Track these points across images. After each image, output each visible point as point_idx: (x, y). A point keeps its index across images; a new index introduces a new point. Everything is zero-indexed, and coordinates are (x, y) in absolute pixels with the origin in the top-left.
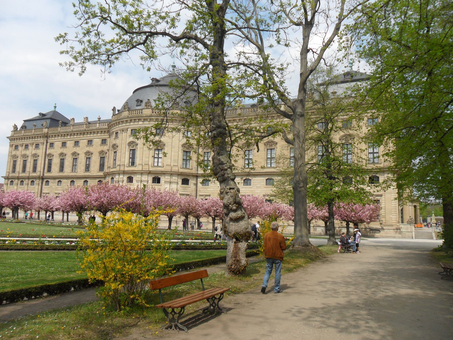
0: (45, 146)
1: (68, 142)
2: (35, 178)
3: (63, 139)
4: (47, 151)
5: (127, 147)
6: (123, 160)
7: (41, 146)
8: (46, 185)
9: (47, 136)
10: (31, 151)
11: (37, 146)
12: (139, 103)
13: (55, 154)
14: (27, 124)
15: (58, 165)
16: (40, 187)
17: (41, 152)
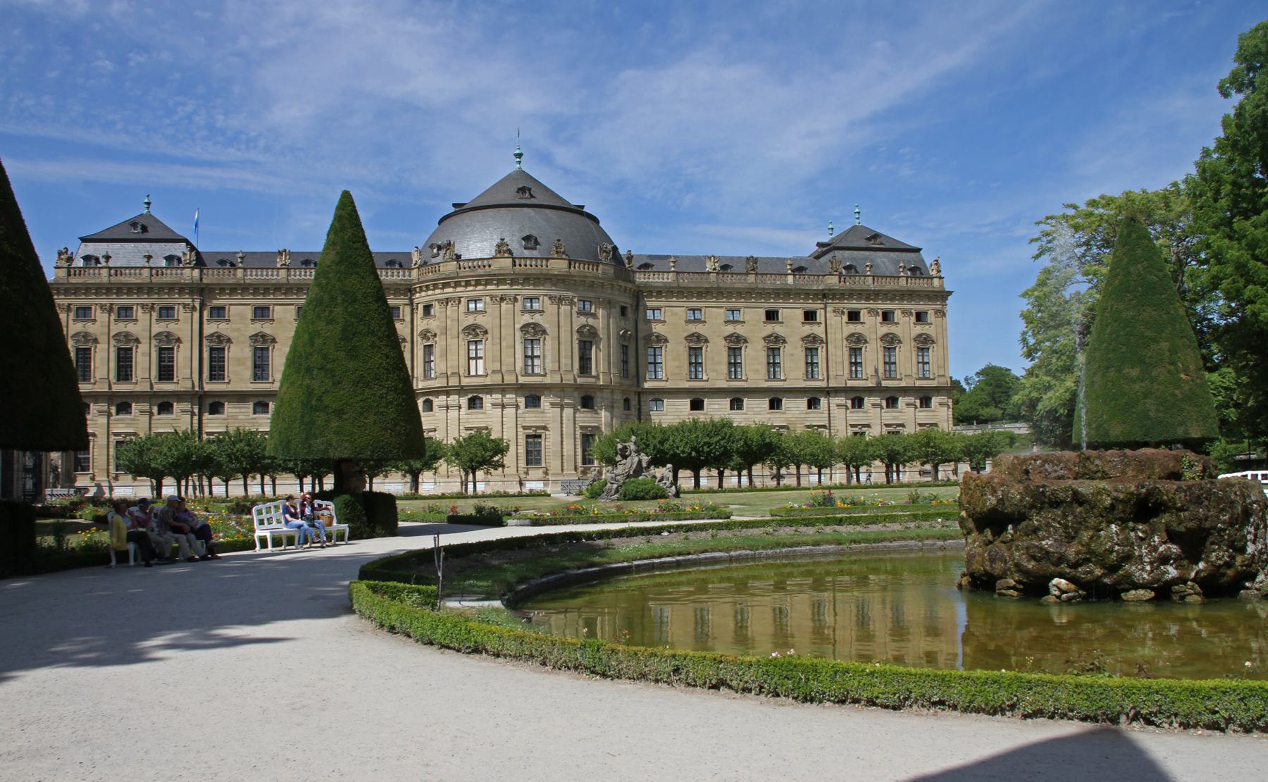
0: (196, 315)
1: (277, 308)
2: (180, 396)
3: (261, 301)
4: (205, 326)
5: (518, 334)
6: (507, 360)
7: (181, 313)
8: (211, 413)
9: (202, 291)
10: (143, 325)
11: (167, 313)
12: (532, 244)
13: (232, 335)
14: (91, 249)
15: (250, 364)
16: (196, 418)
17: (184, 325)
